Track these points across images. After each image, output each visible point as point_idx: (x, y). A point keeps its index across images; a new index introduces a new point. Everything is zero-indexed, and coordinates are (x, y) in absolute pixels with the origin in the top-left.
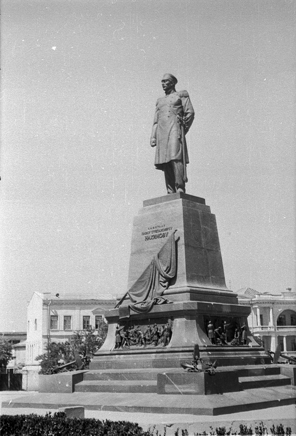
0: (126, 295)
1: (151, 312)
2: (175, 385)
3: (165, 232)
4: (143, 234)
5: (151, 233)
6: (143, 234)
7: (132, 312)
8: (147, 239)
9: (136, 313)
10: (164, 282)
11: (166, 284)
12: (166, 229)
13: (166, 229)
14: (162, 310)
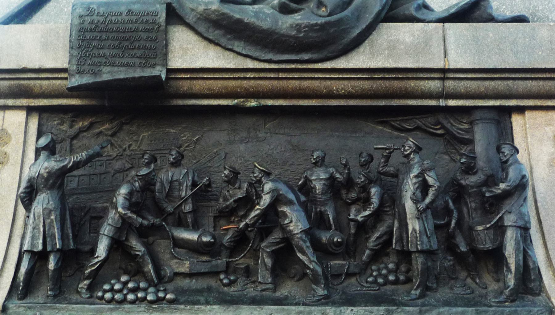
1: (358, 60)
14: (457, 61)
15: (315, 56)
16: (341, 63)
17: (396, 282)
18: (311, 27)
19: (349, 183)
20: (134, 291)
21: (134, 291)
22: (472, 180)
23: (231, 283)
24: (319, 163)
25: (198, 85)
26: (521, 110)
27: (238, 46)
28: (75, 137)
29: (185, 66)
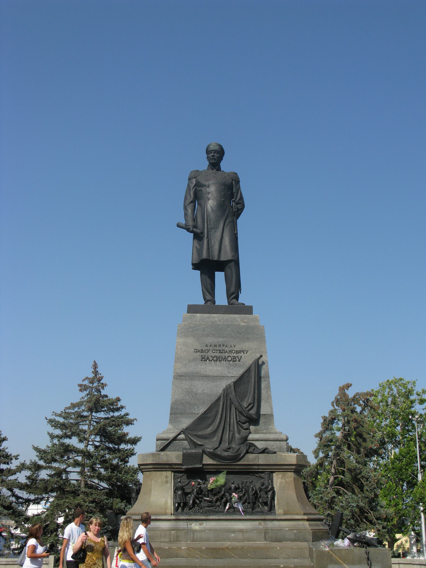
0: (179, 434)
2: (345, 565)
3: (235, 355)
4: (196, 351)
5: (211, 352)
6: (196, 351)
7: (207, 460)
8: (204, 359)
9: (215, 462)
10: (244, 423)
11: (245, 426)
12: (239, 352)
13: (239, 352)
14: (261, 462)
15: (232, 462)
16: (238, 463)
17: (248, 508)
18: (231, 456)
19: (239, 488)
20: (198, 510)
21: (198, 510)
22: (263, 487)
23: (216, 509)
24: (233, 483)
25: (208, 467)
26: (275, 472)
27: (217, 459)
28: (181, 477)
29: (206, 463)
